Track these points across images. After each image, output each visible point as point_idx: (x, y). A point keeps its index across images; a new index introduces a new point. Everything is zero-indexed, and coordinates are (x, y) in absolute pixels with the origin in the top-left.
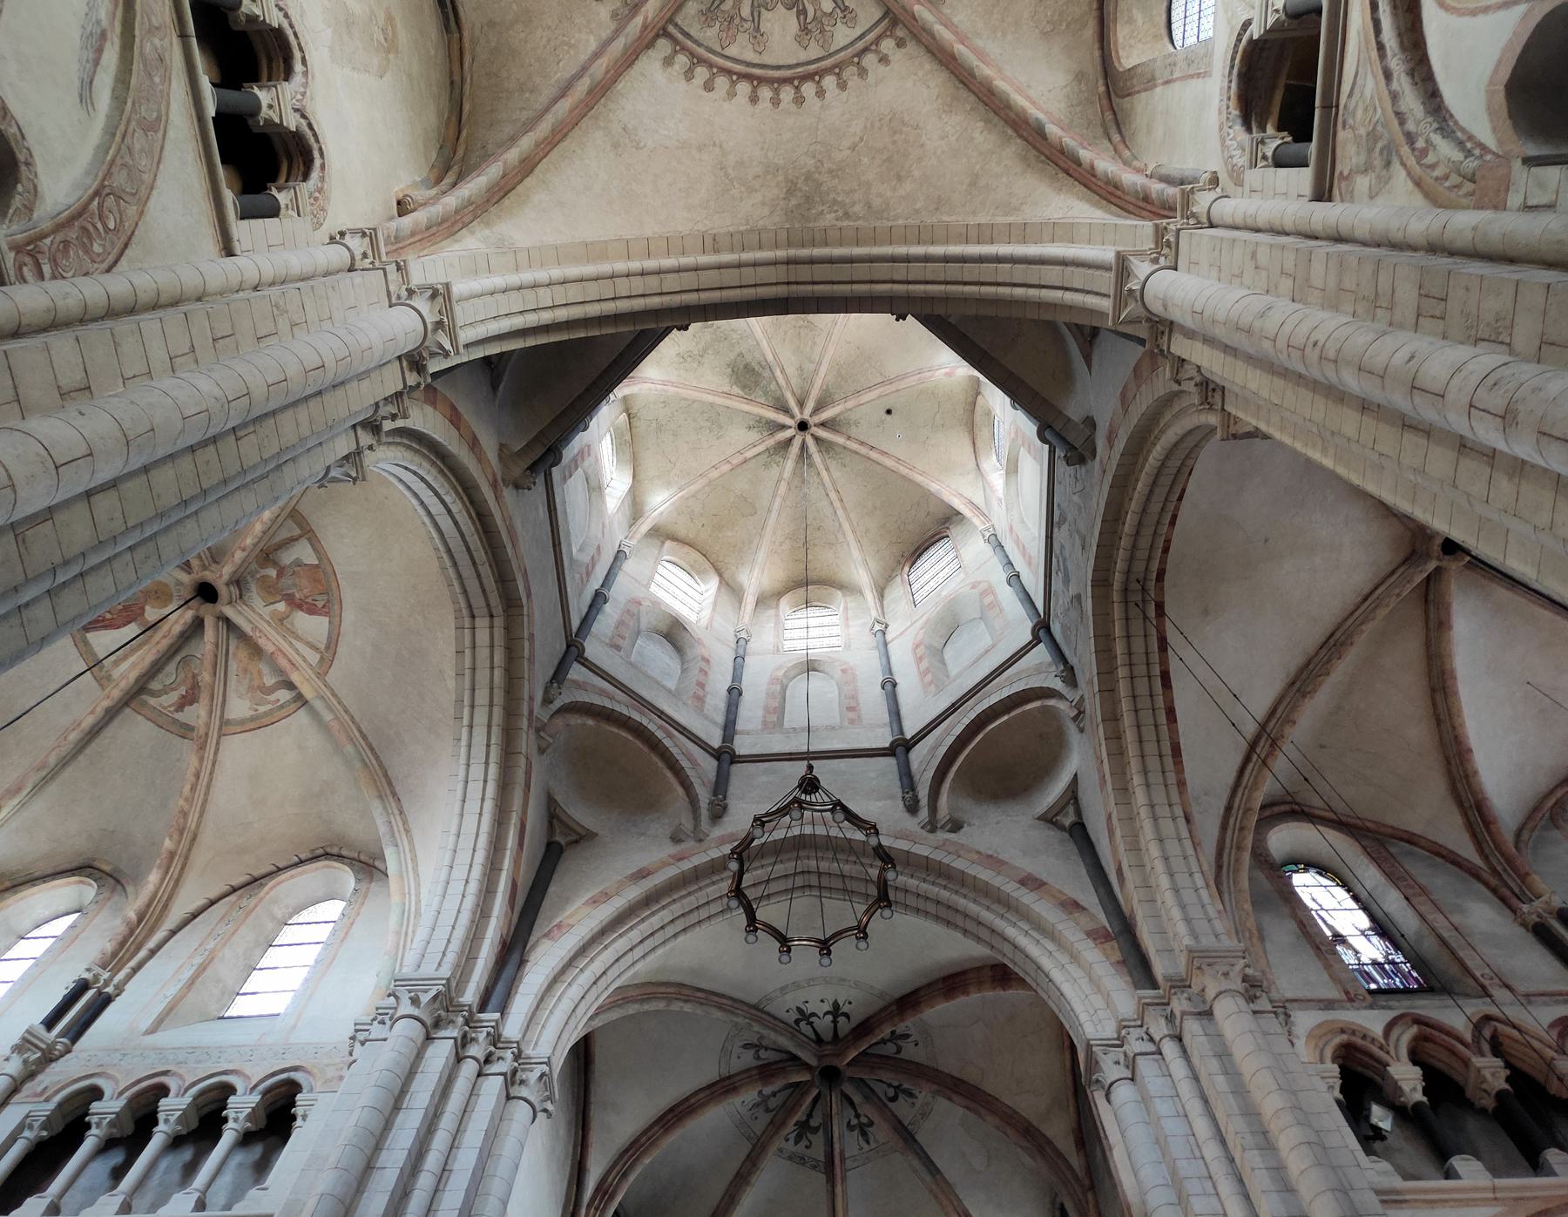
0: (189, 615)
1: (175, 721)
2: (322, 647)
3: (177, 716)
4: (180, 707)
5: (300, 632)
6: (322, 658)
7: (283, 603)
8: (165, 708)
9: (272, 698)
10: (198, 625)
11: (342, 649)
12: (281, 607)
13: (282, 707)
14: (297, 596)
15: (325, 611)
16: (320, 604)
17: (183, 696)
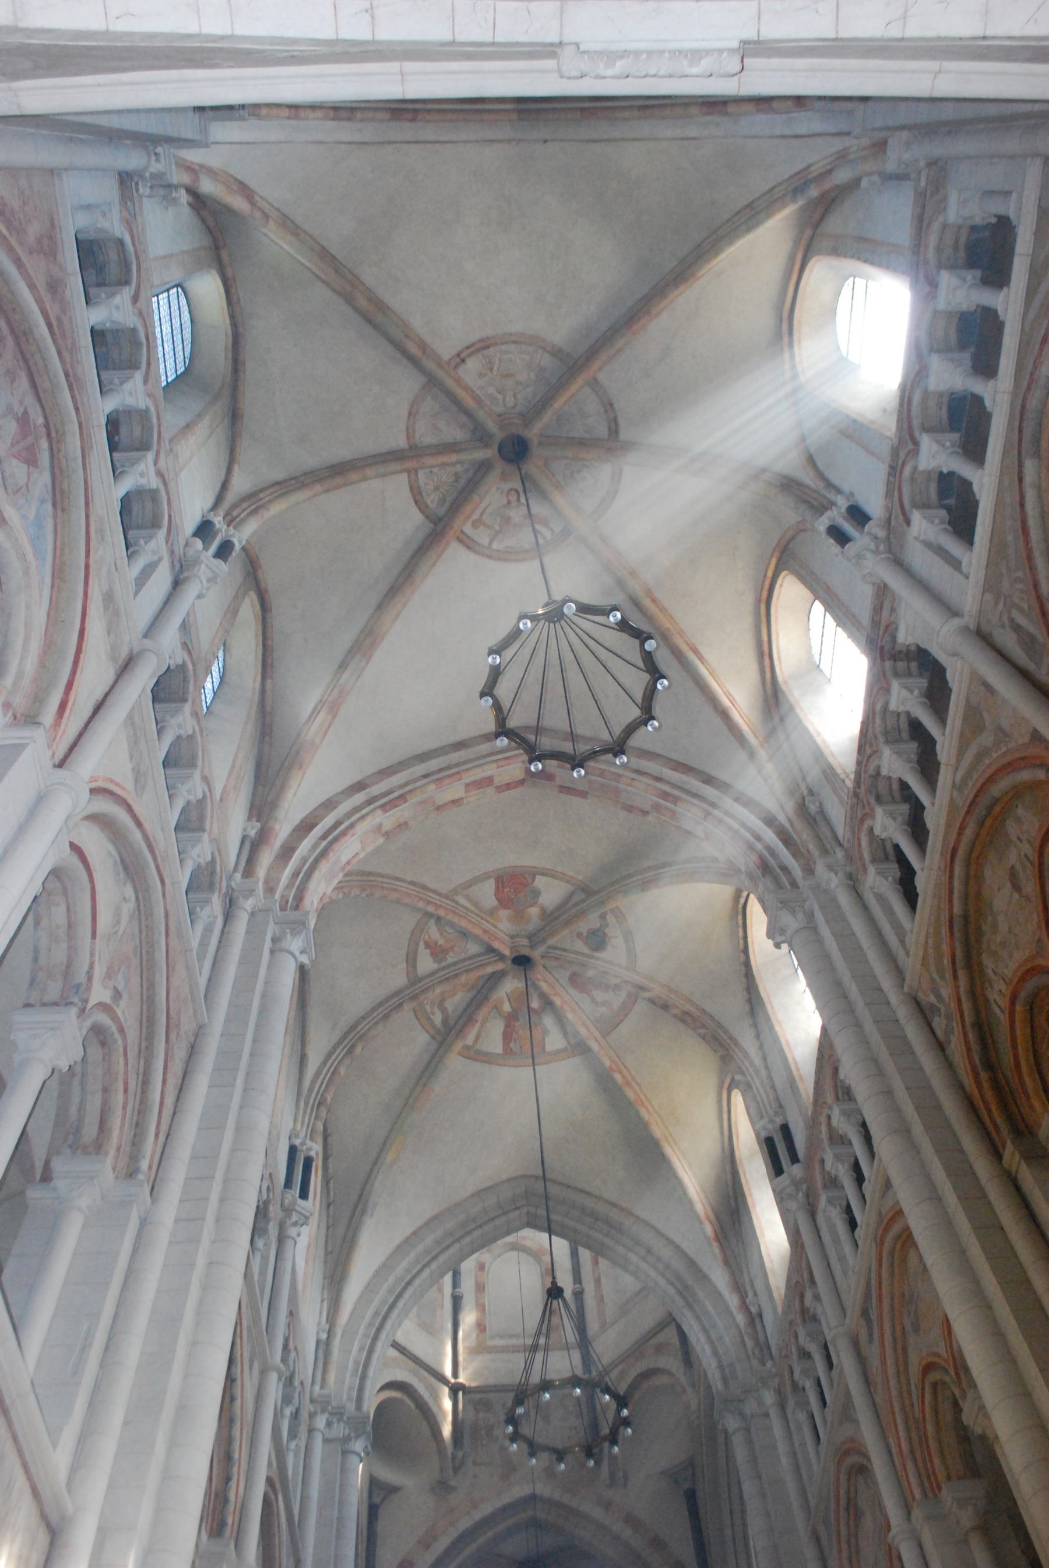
0: (507, 952)
1: (417, 944)
2: (478, 1047)
3: (422, 946)
4: (427, 945)
5: (487, 1024)
6: (467, 1048)
7: (510, 1010)
8: (427, 931)
9: (436, 1009)
10: (502, 957)
11: (478, 1066)
12: (507, 1008)
13: (429, 1019)
14: (517, 1024)
15: (508, 1051)
16: (512, 1045)
17: (436, 943)
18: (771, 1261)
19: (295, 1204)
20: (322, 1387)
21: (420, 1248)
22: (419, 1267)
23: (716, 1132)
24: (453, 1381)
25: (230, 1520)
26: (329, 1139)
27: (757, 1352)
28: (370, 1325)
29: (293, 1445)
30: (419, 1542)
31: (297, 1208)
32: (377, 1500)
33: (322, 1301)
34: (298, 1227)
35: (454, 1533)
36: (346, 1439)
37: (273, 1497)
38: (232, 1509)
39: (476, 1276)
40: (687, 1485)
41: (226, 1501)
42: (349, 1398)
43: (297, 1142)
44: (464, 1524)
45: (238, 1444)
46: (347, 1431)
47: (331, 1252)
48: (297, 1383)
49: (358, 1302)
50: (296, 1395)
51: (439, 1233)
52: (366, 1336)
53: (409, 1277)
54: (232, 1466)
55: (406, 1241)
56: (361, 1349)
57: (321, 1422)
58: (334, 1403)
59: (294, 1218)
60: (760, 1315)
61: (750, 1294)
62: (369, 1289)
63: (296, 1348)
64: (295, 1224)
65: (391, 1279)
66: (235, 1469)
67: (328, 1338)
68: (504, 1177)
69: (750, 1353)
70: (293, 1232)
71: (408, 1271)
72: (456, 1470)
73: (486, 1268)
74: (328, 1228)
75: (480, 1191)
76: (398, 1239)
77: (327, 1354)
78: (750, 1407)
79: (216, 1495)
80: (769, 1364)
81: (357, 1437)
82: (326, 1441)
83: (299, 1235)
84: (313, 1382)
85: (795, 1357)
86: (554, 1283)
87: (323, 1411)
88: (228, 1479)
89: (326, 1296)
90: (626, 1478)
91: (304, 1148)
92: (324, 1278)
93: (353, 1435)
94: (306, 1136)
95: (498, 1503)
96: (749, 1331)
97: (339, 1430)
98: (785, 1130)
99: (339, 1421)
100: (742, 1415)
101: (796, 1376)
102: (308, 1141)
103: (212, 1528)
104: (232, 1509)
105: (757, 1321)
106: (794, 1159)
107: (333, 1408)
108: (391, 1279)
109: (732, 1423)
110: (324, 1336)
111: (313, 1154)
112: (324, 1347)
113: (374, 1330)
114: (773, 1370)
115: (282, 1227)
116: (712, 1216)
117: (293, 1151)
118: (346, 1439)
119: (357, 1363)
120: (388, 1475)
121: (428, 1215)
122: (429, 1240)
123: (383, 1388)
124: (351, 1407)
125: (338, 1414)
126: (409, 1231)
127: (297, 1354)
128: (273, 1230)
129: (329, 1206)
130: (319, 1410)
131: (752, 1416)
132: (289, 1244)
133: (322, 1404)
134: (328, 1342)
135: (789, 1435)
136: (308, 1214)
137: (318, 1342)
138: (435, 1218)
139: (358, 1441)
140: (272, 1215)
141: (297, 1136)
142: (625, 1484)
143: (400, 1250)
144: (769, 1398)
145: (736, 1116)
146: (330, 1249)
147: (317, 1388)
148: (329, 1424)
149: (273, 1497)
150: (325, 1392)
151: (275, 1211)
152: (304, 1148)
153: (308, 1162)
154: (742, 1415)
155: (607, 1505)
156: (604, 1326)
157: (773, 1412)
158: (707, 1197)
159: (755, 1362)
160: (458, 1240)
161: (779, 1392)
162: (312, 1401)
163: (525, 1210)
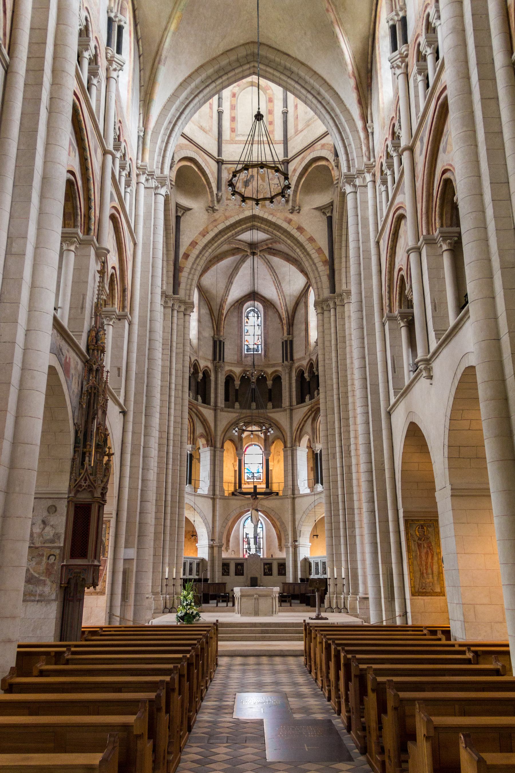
18: (383, 103)
19: (114, 57)
20: (142, 161)
21: (193, 85)
22: (193, 96)
23: (367, 20)
24: (217, 158)
25: (93, 228)
26: (137, 12)
27: (367, 154)
28: (167, 129)
29: (128, 190)
30: (200, 234)
31: (115, 59)
32: (180, 214)
33: (140, 114)
34: (117, 71)
35: (216, 231)
36: (156, 188)
37: (118, 215)
38: (93, 222)
39: (231, 101)
40: (328, 215)
41: (89, 218)
42: (157, 168)
43: (112, 15)
44: (221, 227)
45: (93, 192)
46: (157, 184)
47: (143, 86)
48: (127, 159)
49: (160, 116)
50: (128, 165)
51: (204, 76)
52: (165, 134)
53: (188, 102)
54: (91, 202)
55: (185, 81)
56: (163, 141)
57: (143, 179)
58: (149, 170)
59: (114, 66)
60: (373, 133)
61: (369, 121)
62: (166, 108)
63: (125, 141)
64: (115, 70)
65: (178, 103)
66: (93, 204)
67: (144, 135)
68: (242, 42)
69: (364, 154)
70: (114, 74)
71: (186, 98)
72: (219, 201)
73: (236, 96)
74: (140, 71)
75: (227, 51)
76: (180, 80)
77: (144, 143)
78: (358, 182)
79: (85, 216)
81: (162, 187)
82: (145, 188)
83: (118, 77)
84: (137, 159)
85: (385, 158)
86: (259, 113)
87: (144, 173)
88: (90, 208)
89: (141, 112)
90: (300, 210)
91: (117, 19)
92: (140, 101)
93: (159, 186)
94: (118, 11)
95: (237, 218)
96: (365, 142)
97: (153, 183)
99: (152, 178)
100: (355, 186)
101: (384, 168)
102: (119, 15)
103: (84, 232)
104: (93, 222)
105: (370, 137)
107: (149, 172)
108: (178, 103)
109: (348, 189)
110: (142, 134)
111: (122, 23)
112: (142, 140)
113: (169, 131)
114: (374, 163)
115: (107, 70)
116: (356, 75)
117: (110, 21)
118: (156, 188)
119: (160, 149)
120: (185, 202)
121: (197, 66)
122: (198, 80)
123: (181, 160)
124: (158, 173)
125: (151, 175)
126: (187, 75)
127: (126, 143)
128: (102, 73)
129: (140, 57)
130: (141, 173)
131: (359, 186)
132: (113, 82)
133: (142, 169)
134: (144, 138)
135: (375, 197)
136: (122, 64)
137: (139, 137)
138: (202, 66)
139: (162, 189)
140: (100, 64)
141: (112, 11)
142: (299, 212)
143: (183, 85)
144: (369, 177)
145: (381, 8)
146: (142, 84)
147: (139, 161)
148: (147, 180)
149: (118, 215)
150: (143, 164)
151: (103, 62)
152: (117, 19)
153: (120, 29)
154: (355, 186)
155: (289, 222)
156: (297, 132)
157: (370, 185)
158: (355, 61)
159: (365, 159)
160: (213, 81)
161: (374, 175)
162: (137, 168)
163: (252, 64)
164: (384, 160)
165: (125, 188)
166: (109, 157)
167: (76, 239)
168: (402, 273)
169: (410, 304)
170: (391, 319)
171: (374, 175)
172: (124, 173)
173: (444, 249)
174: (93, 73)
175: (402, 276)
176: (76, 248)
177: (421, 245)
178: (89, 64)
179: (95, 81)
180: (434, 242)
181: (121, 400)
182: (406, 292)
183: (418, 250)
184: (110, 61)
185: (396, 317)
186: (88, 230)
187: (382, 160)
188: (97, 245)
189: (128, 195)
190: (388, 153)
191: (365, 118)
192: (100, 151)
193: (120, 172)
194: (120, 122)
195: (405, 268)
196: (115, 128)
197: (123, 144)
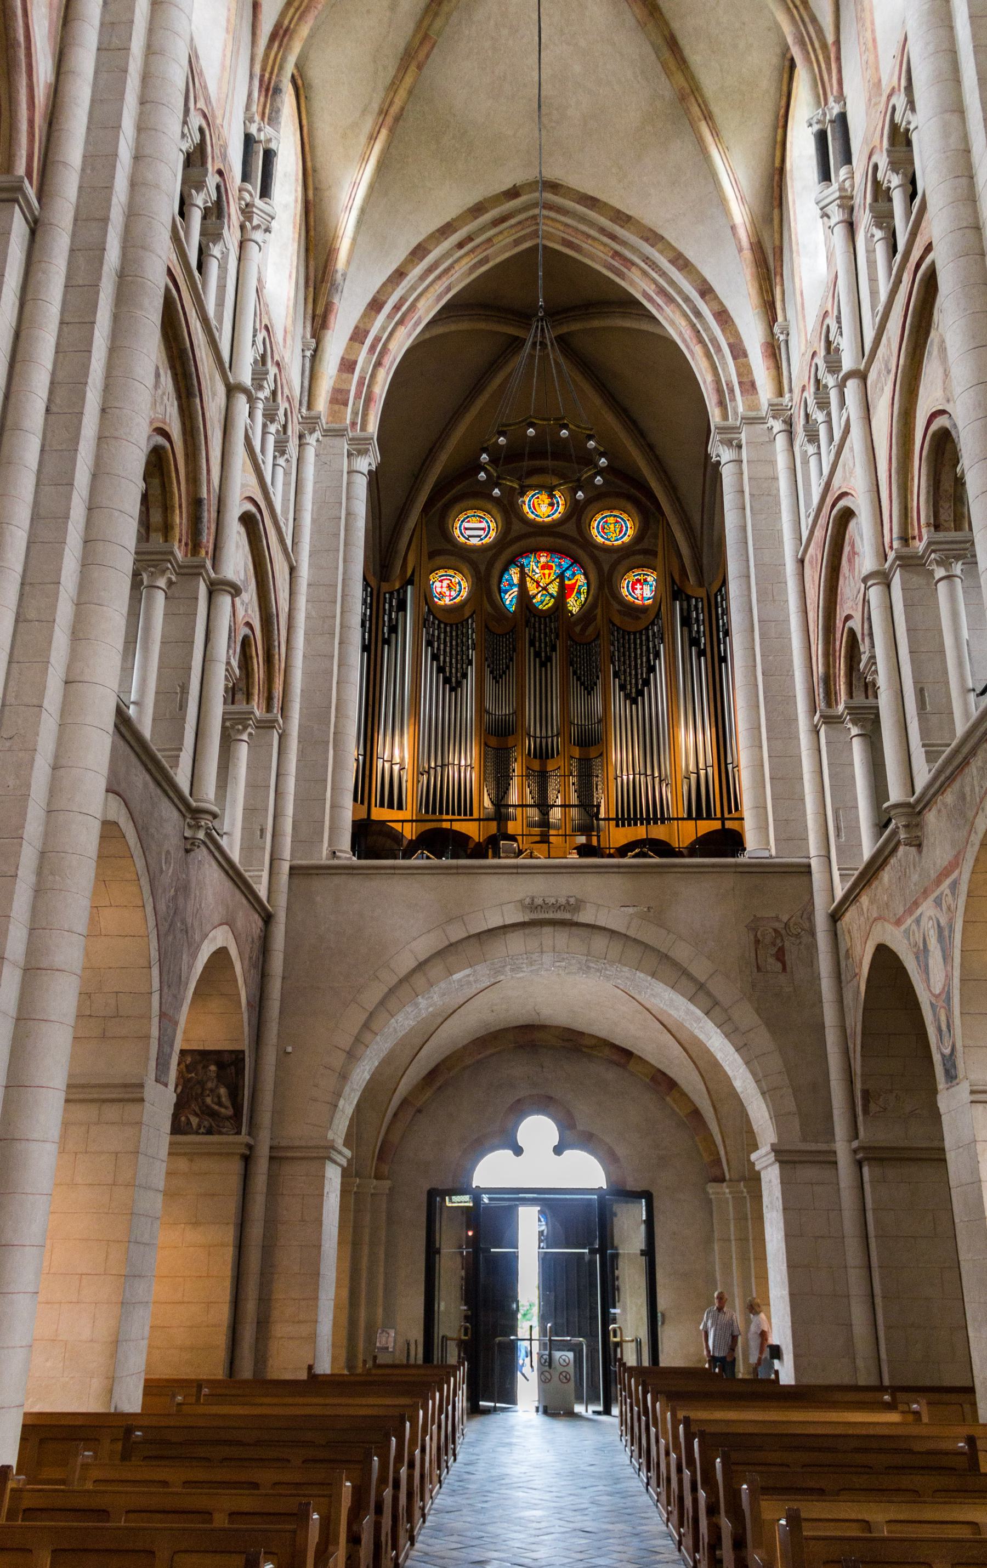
29: (281, 461)
57: (311, 439)
63: (278, 364)
80: (787, 396)
98: (842, 119)
106: (847, 158)
164: (810, 395)
165: (275, 457)
166: (241, 400)
167: (169, 566)
168: (849, 624)
169: (870, 689)
170: (830, 720)
171: (789, 423)
172: (273, 428)
173: (937, 577)
174: (211, 234)
175: (852, 632)
176: (170, 583)
177: (891, 566)
178: (204, 218)
179: (216, 250)
180: (919, 562)
181: (263, 893)
182: (862, 666)
183: (884, 578)
184: (247, 211)
185: (840, 717)
186: (195, 546)
187: (806, 394)
188: (213, 575)
189: (280, 472)
190: (818, 381)
191: (769, 309)
192: (221, 389)
193: (265, 426)
194: (267, 328)
195: (857, 616)
196: (254, 342)
197: (273, 370)
